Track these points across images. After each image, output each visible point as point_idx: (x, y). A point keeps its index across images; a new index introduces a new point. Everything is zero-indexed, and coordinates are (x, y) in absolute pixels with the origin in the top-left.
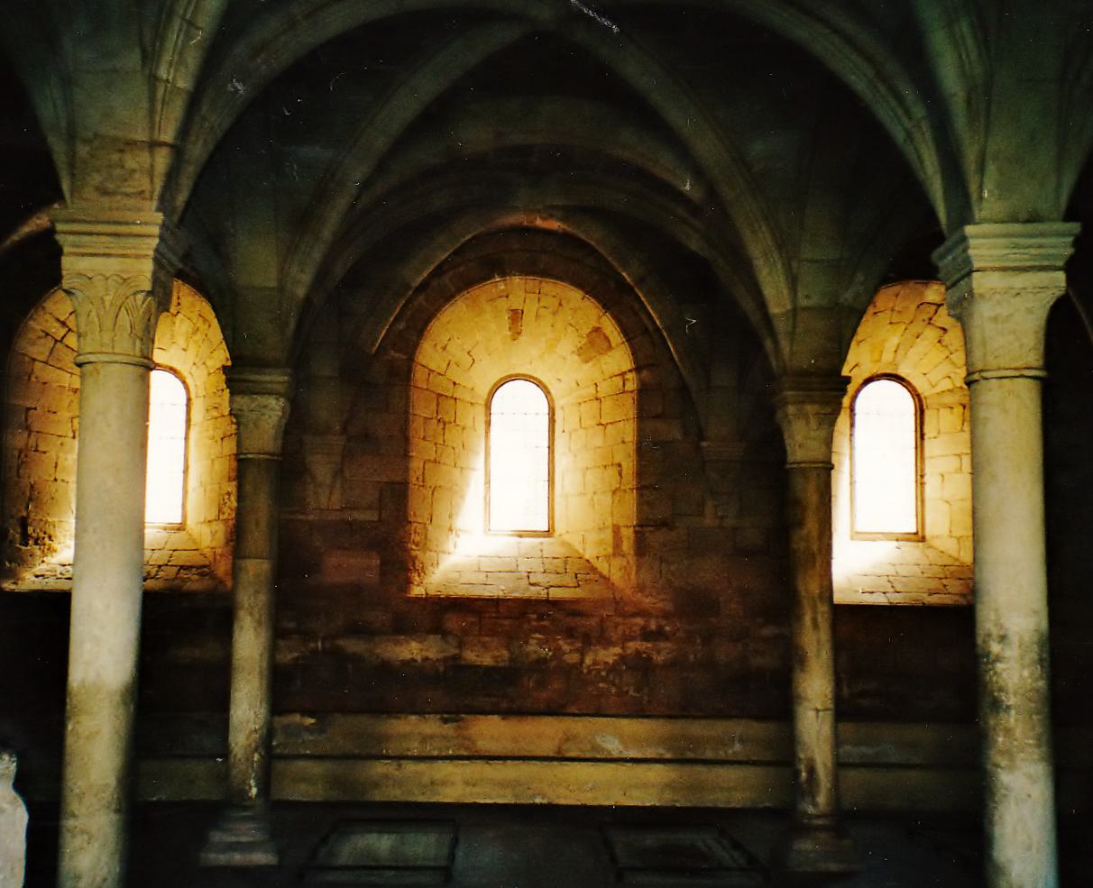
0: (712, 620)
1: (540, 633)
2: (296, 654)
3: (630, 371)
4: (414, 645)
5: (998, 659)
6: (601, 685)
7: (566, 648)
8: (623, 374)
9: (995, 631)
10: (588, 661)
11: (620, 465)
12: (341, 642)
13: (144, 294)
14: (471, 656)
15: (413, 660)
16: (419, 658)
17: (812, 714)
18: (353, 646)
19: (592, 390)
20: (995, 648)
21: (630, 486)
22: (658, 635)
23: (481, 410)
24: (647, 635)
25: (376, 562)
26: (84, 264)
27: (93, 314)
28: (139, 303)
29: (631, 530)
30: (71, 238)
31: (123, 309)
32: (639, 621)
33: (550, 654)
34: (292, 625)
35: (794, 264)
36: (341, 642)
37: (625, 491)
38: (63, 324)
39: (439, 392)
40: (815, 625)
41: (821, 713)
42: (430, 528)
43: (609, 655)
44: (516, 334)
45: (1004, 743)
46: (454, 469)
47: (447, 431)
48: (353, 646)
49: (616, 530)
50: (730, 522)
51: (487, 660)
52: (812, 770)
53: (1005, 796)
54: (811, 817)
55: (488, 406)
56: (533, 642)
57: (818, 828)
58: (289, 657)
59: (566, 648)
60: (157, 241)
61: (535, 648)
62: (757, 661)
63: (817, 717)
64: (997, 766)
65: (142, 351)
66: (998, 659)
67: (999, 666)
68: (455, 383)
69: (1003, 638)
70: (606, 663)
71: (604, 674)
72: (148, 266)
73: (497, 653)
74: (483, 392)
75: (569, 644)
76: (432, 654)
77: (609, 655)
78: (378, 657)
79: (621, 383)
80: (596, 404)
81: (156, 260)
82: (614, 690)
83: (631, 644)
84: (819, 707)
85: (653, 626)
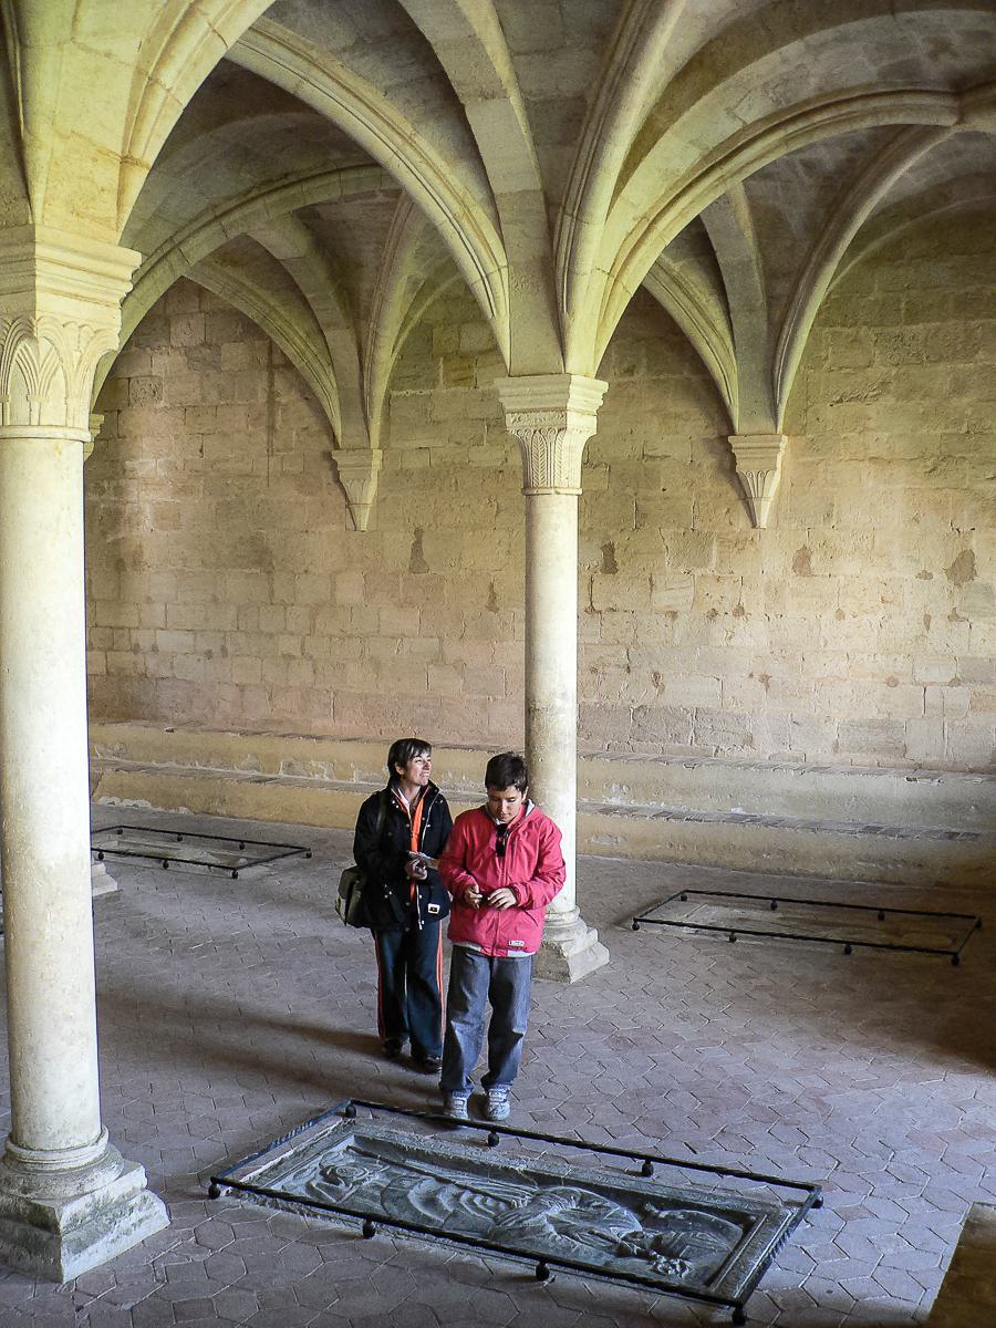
27: (60, 372)
30: (53, 268)
67: (561, 716)
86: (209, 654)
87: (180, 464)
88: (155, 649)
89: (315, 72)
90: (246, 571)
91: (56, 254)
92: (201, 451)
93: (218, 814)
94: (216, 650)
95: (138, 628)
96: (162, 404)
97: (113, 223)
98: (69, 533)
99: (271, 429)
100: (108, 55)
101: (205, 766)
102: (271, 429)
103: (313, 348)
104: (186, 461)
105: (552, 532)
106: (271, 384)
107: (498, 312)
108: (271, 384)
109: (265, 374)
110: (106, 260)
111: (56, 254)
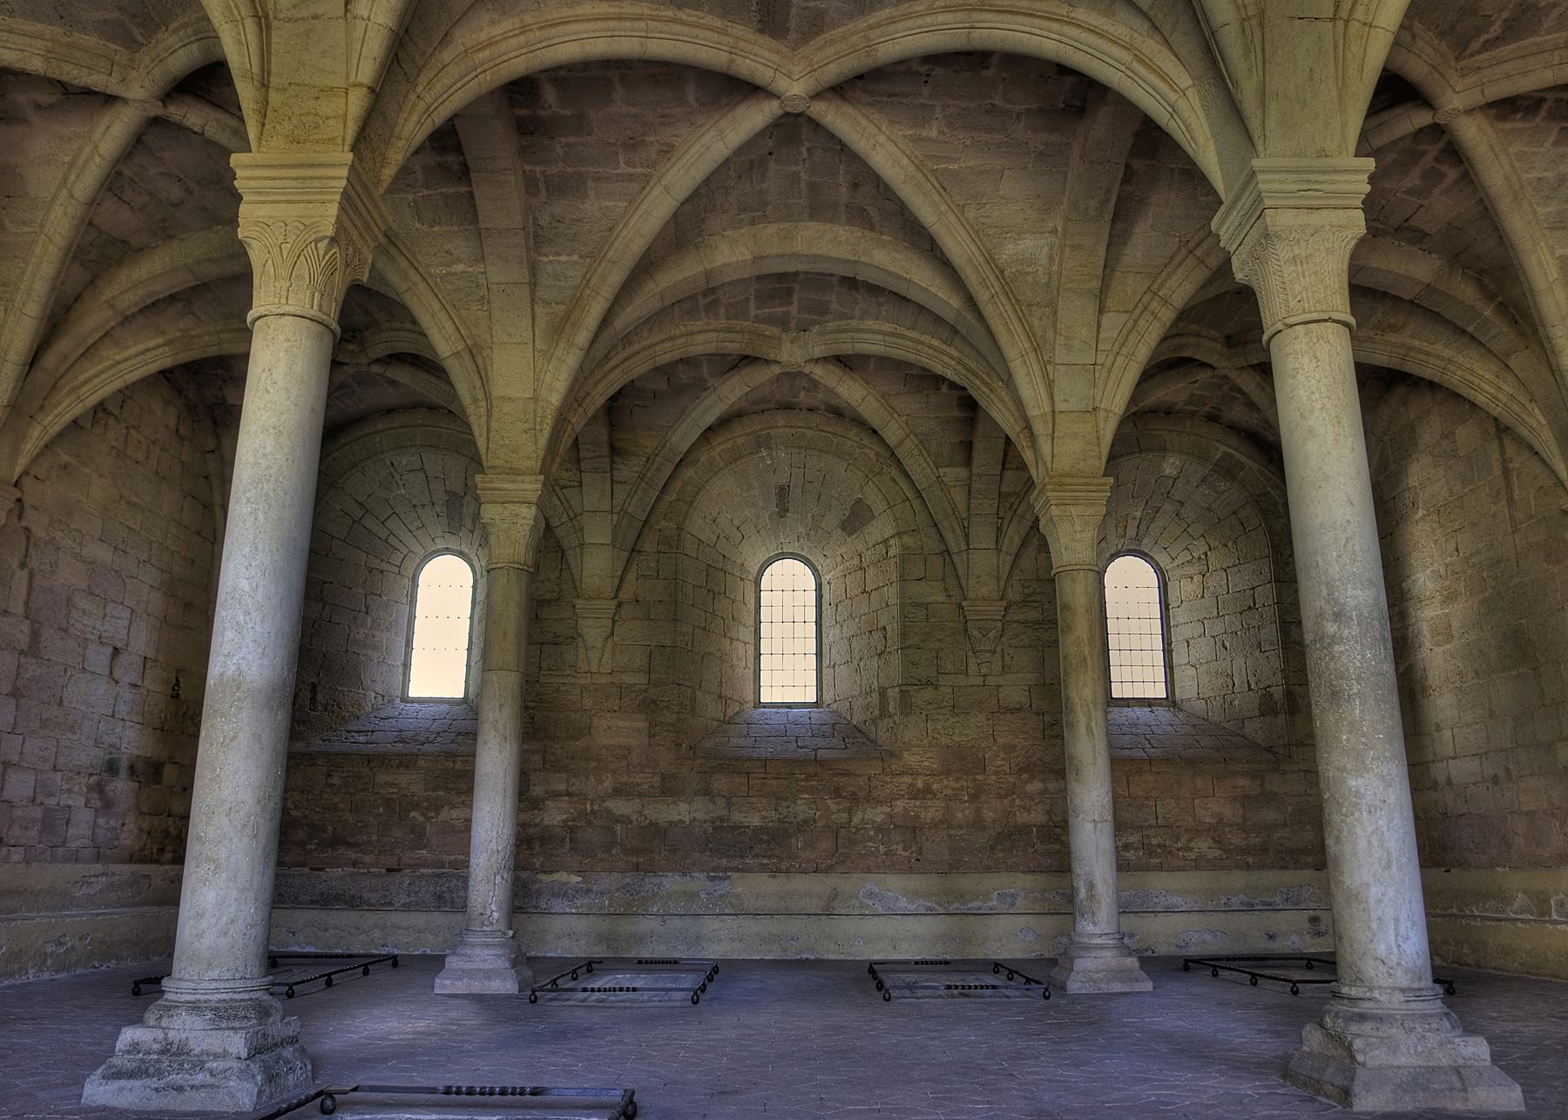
0: (980, 777)
1: (808, 793)
2: (565, 817)
3: (893, 537)
4: (683, 807)
5: (1334, 640)
6: (870, 844)
7: (834, 807)
8: (886, 541)
9: (1328, 610)
10: (856, 820)
11: (884, 628)
12: (610, 804)
13: (326, 241)
14: (738, 817)
15: (682, 821)
16: (687, 819)
17: (1090, 826)
18: (619, 807)
19: (856, 561)
20: (1331, 628)
21: (896, 648)
22: (927, 792)
23: (750, 588)
24: (915, 794)
25: (643, 725)
26: (264, 211)
28: (322, 252)
29: (897, 689)
31: (302, 257)
32: (907, 779)
33: (818, 813)
34: (562, 787)
35: (1050, 368)
36: (610, 804)
37: (890, 652)
38: (361, 504)
39: (710, 563)
40: (1089, 728)
41: (1099, 825)
42: (698, 693)
43: (878, 814)
44: (783, 511)
45: (1348, 740)
46: (723, 639)
47: (716, 601)
48: (619, 807)
49: (882, 693)
50: (992, 681)
51: (755, 821)
52: (1091, 886)
53: (1356, 805)
54: (1092, 936)
55: (758, 582)
56: (799, 802)
57: (1102, 947)
58: (559, 818)
59: (834, 807)
60: (344, 182)
61: (802, 809)
62: (1022, 818)
63: (1095, 828)
64: (1343, 769)
65: (320, 306)
66: (1334, 640)
68: (724, 556)
69: (1338, 616)
70: (874, 822)
71: (871, 833)
72: (333, 210)
73: (763, 813)
74: (754, 570)
75: (837, 803)
76: (699, 815)
77: (878, 814)
78: (646, 818)
79: (884, 551)
80: (860, 573)
81: (342, 207)
82: (882, 849)
83: (898, 803)
84: (1097, 819)
85: (920, 785)
86: (1495, 780)
87: (1442, 572)
88: (1449, 782)
89: (976, 16)
90: (1514, 672)
91: (249, 173)
92: (1457, 549)
93: (1467, 965)
94: (1502, 774)
95: (1433, 762)
96: (1421, 513)
97: (339, 141)
98: (268, 392)
99: (1511, 501)
100: (315, 17)
101: (1483, 912)
102: (1511, 501)
103: (1505, 387)
104: (1447, 565)
105: (1290, 381)
106: (1503, 452)
107: (1196, 144)
108: (1503, 452)
109: (1495, 445)
110: (312, 166)
111: (249, 173)
